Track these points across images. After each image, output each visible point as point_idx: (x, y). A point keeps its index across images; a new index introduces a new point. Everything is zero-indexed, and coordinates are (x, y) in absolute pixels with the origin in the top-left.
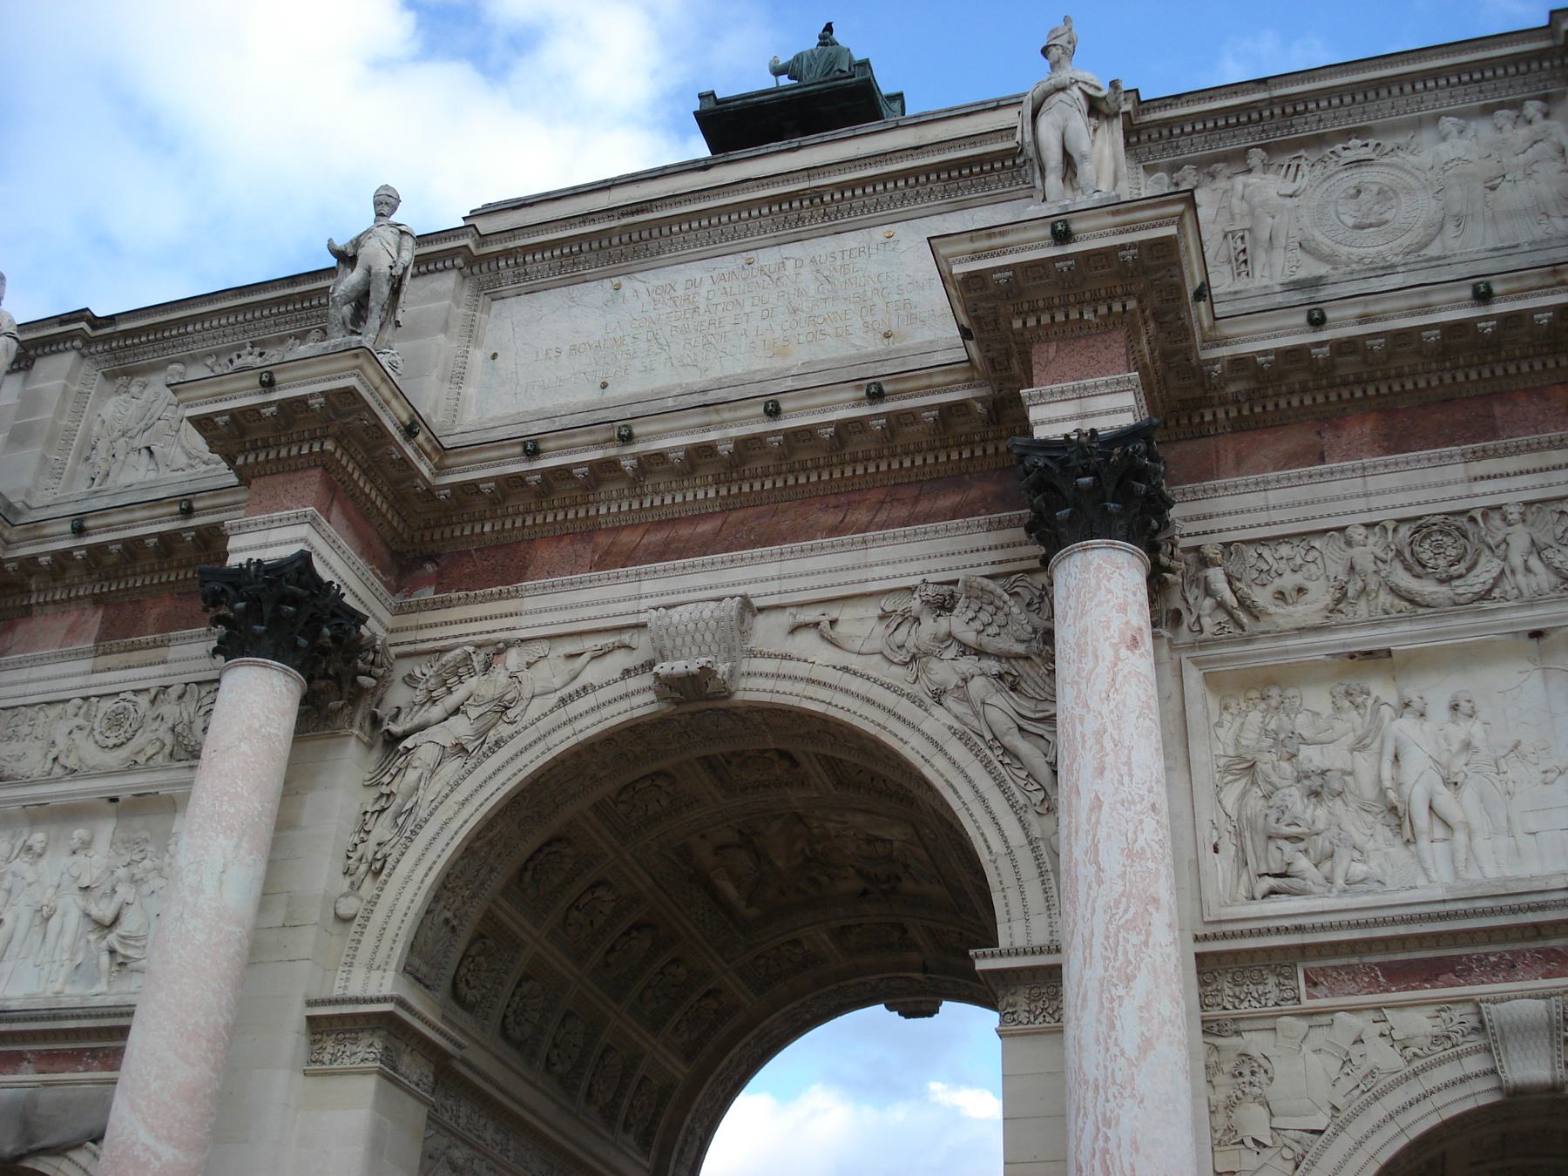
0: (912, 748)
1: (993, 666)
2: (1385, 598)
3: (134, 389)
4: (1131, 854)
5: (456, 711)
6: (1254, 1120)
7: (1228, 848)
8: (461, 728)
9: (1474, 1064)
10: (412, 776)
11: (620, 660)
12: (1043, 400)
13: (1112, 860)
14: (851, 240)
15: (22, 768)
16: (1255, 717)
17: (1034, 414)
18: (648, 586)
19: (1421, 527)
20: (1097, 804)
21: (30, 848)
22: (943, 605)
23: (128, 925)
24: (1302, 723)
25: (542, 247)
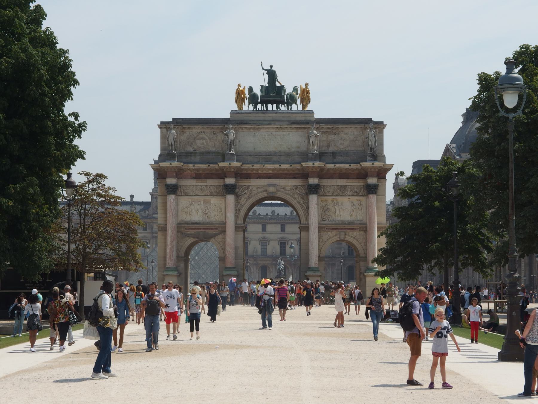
0: (293, 203)
1: (301, 196)
2: (337, 193)
3: (185, 135)
4: (315, 224)
5: (245, 194)
6: (321, 240)
7: (321, 216)
8: (246, 196)
9: (338, 237)
10: (241, 201)
11: (262, 189)
12: (310, 179)
13: (314, 224)
14: (284, 133)
15: (190, 194)
16: (324, 203)
17: (309, 180)
18: (265, 181)
19: (341, 186)
20: (313, 219)
21: (192, 204)
22: (296, 189)
23: (209, 214)
24: (328, 204)
25: (245, 128)
